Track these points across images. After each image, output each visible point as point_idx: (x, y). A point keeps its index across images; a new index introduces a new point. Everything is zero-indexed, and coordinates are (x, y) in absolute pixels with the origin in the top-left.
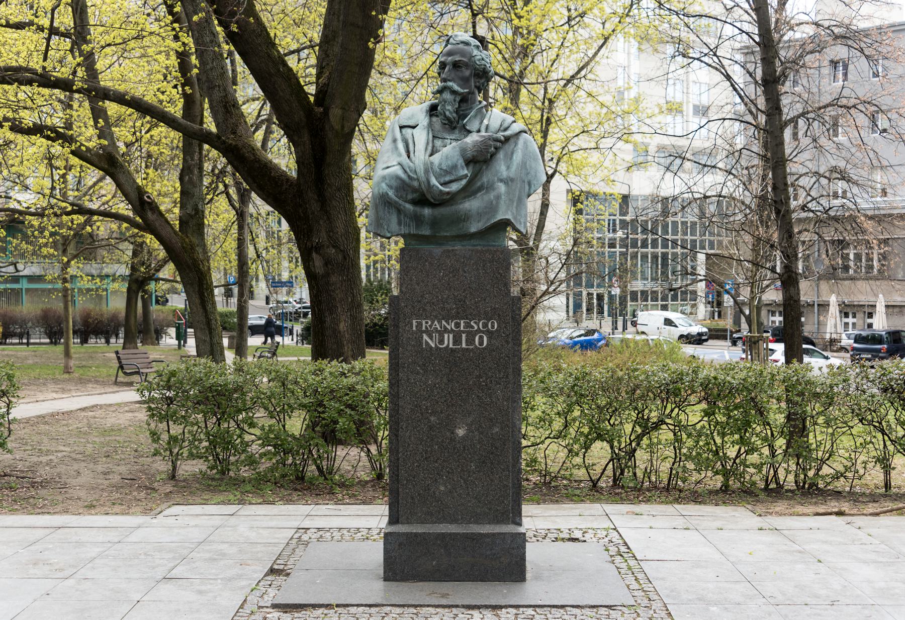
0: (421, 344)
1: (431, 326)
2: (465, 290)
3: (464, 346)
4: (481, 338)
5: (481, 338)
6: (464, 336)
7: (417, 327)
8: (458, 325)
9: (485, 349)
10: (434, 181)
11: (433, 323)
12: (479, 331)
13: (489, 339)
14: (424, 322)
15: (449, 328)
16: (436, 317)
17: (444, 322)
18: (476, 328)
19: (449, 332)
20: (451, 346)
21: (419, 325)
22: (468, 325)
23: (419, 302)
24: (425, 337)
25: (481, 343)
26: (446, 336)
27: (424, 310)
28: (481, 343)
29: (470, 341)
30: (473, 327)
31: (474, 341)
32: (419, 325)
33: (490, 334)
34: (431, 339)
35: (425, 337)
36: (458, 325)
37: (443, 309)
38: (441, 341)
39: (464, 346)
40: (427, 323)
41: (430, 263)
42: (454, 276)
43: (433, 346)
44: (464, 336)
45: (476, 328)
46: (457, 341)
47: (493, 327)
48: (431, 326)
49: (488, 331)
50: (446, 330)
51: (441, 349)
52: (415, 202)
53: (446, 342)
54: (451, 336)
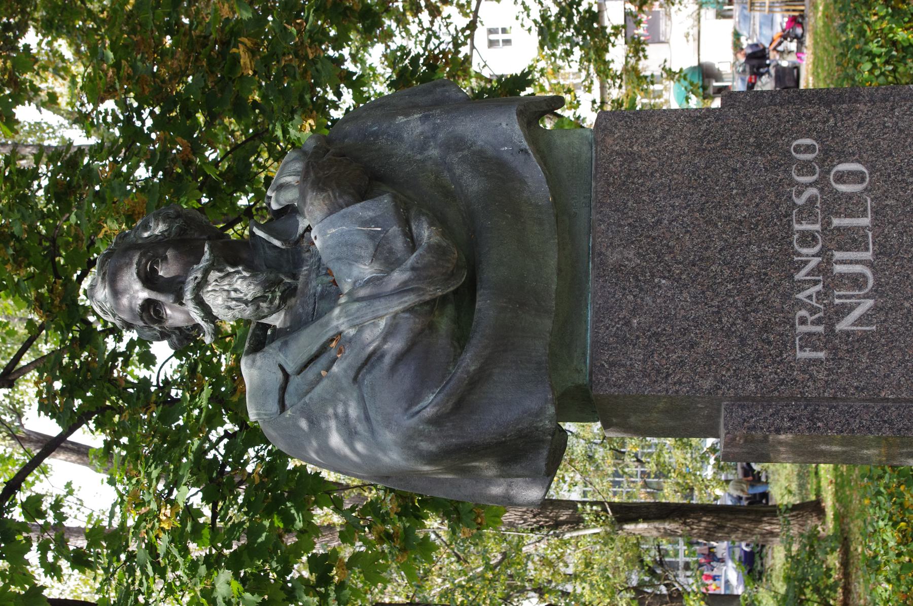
0: (865, 336)
1: (813, 311)
2: (709, 222)
3: (865, 221)
4: (841, 178)
5: (841, 178)
6: (836, 222)
7: (815, 349)
8: (807, 239)
9: (872, 169)
10: (398, 277)
11: (803, 305)
12: (822, 184)
13: (844, 157)
14: (801, 329)
15: (815, 261)
16: (786, 296)
17: (800, 275)
18: (814, 191)
19: (829, 261)
20: (868, 255)
21: (809, 340)
22: (807, 213)
23: (743, 341)
24: (844, 325)
25: (858, 177)
26: (838, 269)
27: (765, 328)
28: (858, 177)
29: (851, 205)
30: (812, 201)
31: (850, 196)
32: (809, 340)
33: (828, 156)
34: (851, 309)
35: (844, 325)
36: (807, 239)
37: (762, 278)
38: (857, 281)
39: (865, 221)
40: (803, 321)
41: (634, 312)
42: (671, 250)
43: (870, 303)
44: (836, 222)
45: (814, 191)
46: (851, 240)
47: (809, 149)
48: (813, 311)
49: (822, 162)
50: (824, 270)
51: (878, 284)
52: (461, 339)
53: (858, 268)
54: (838, 255)
